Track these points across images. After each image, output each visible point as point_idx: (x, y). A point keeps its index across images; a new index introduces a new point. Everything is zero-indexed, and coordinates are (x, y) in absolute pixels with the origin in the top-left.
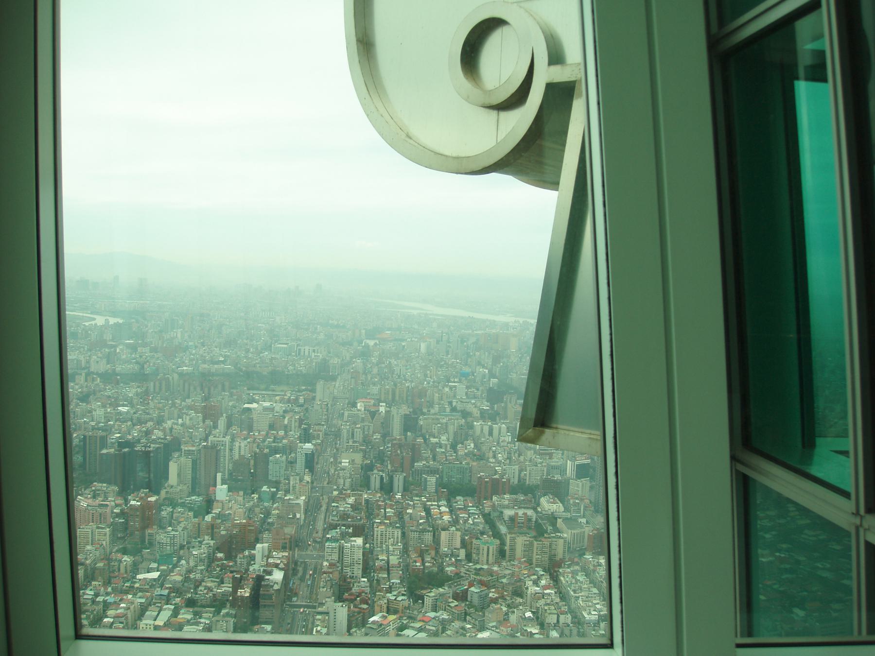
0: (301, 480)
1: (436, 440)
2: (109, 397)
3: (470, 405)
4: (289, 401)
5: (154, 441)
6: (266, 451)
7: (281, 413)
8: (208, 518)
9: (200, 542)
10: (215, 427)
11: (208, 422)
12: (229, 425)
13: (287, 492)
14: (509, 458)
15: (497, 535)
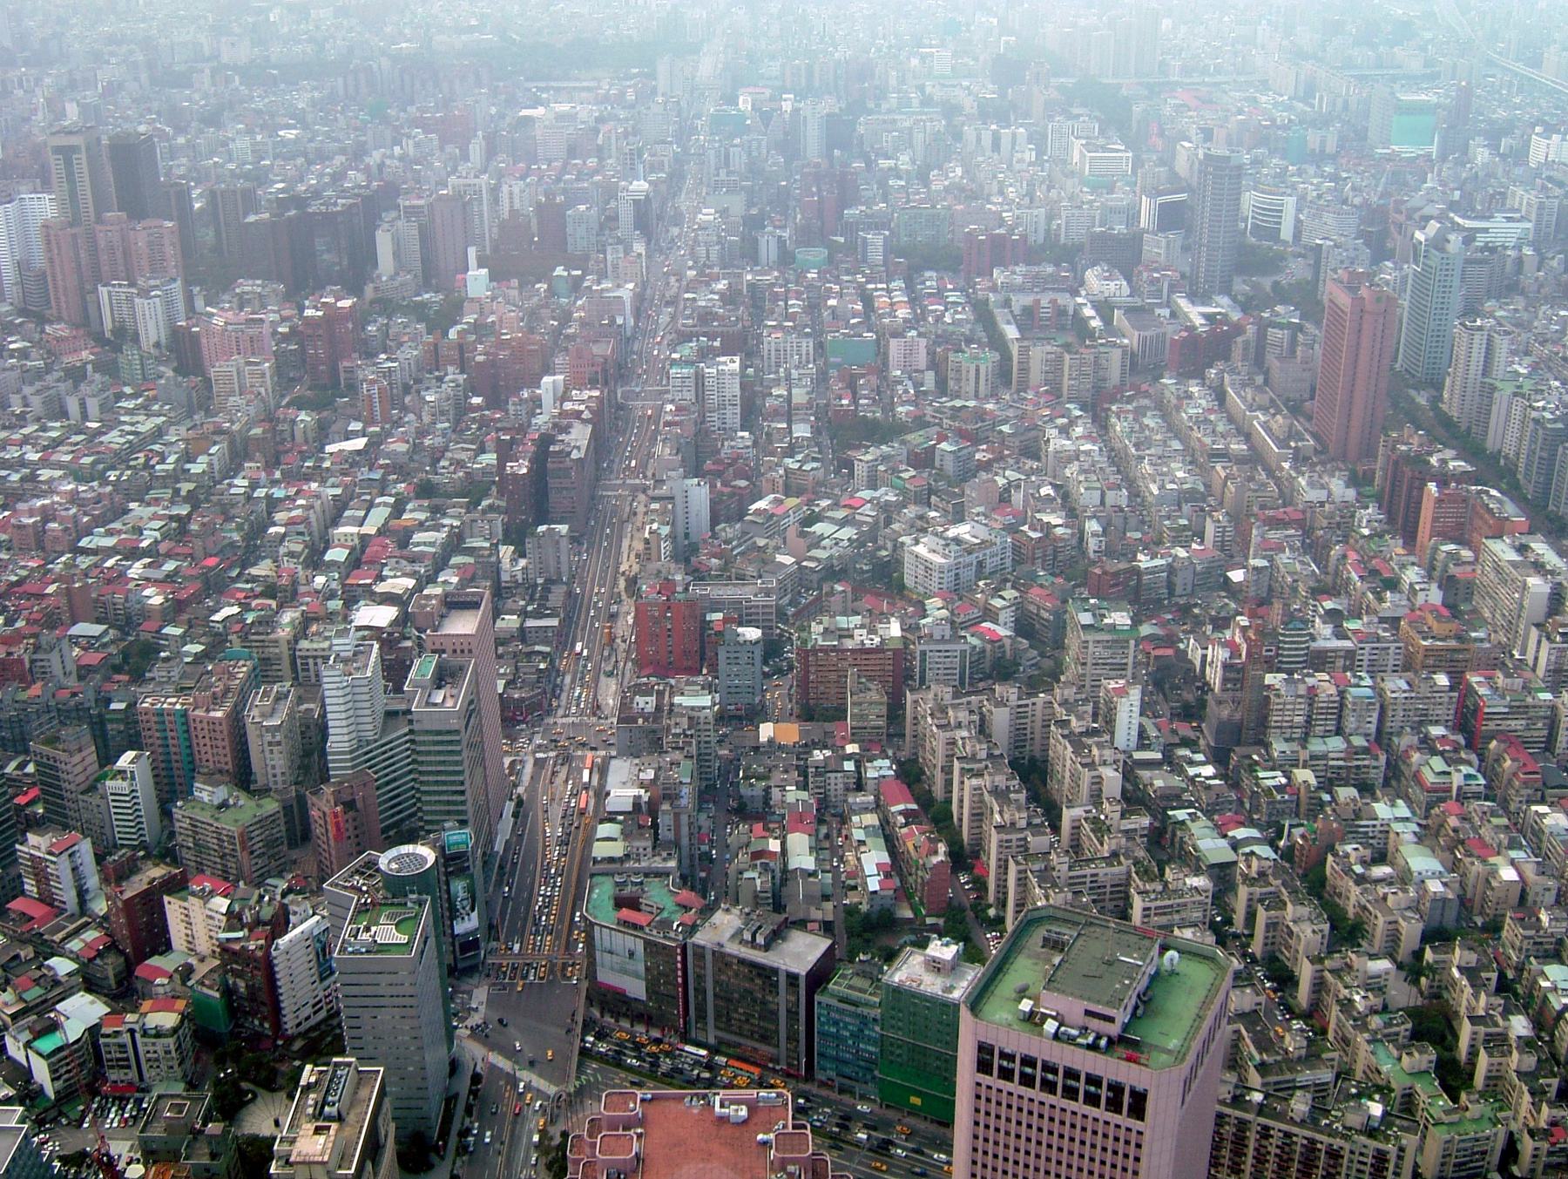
0: (628, 250)
1: (891, 163)
2: (259, 112)
3: (957, 91)
4: (606, 99)
5: (343, 193)
6: (560, 199)
7: (592, 124)
8: (453, 334)
9: (440, 379)
10: (465, 157)
11: (449, 148)
12: (491, 153)
13: (602, 276)
14: (1030, 195)
15: (997, 341)
